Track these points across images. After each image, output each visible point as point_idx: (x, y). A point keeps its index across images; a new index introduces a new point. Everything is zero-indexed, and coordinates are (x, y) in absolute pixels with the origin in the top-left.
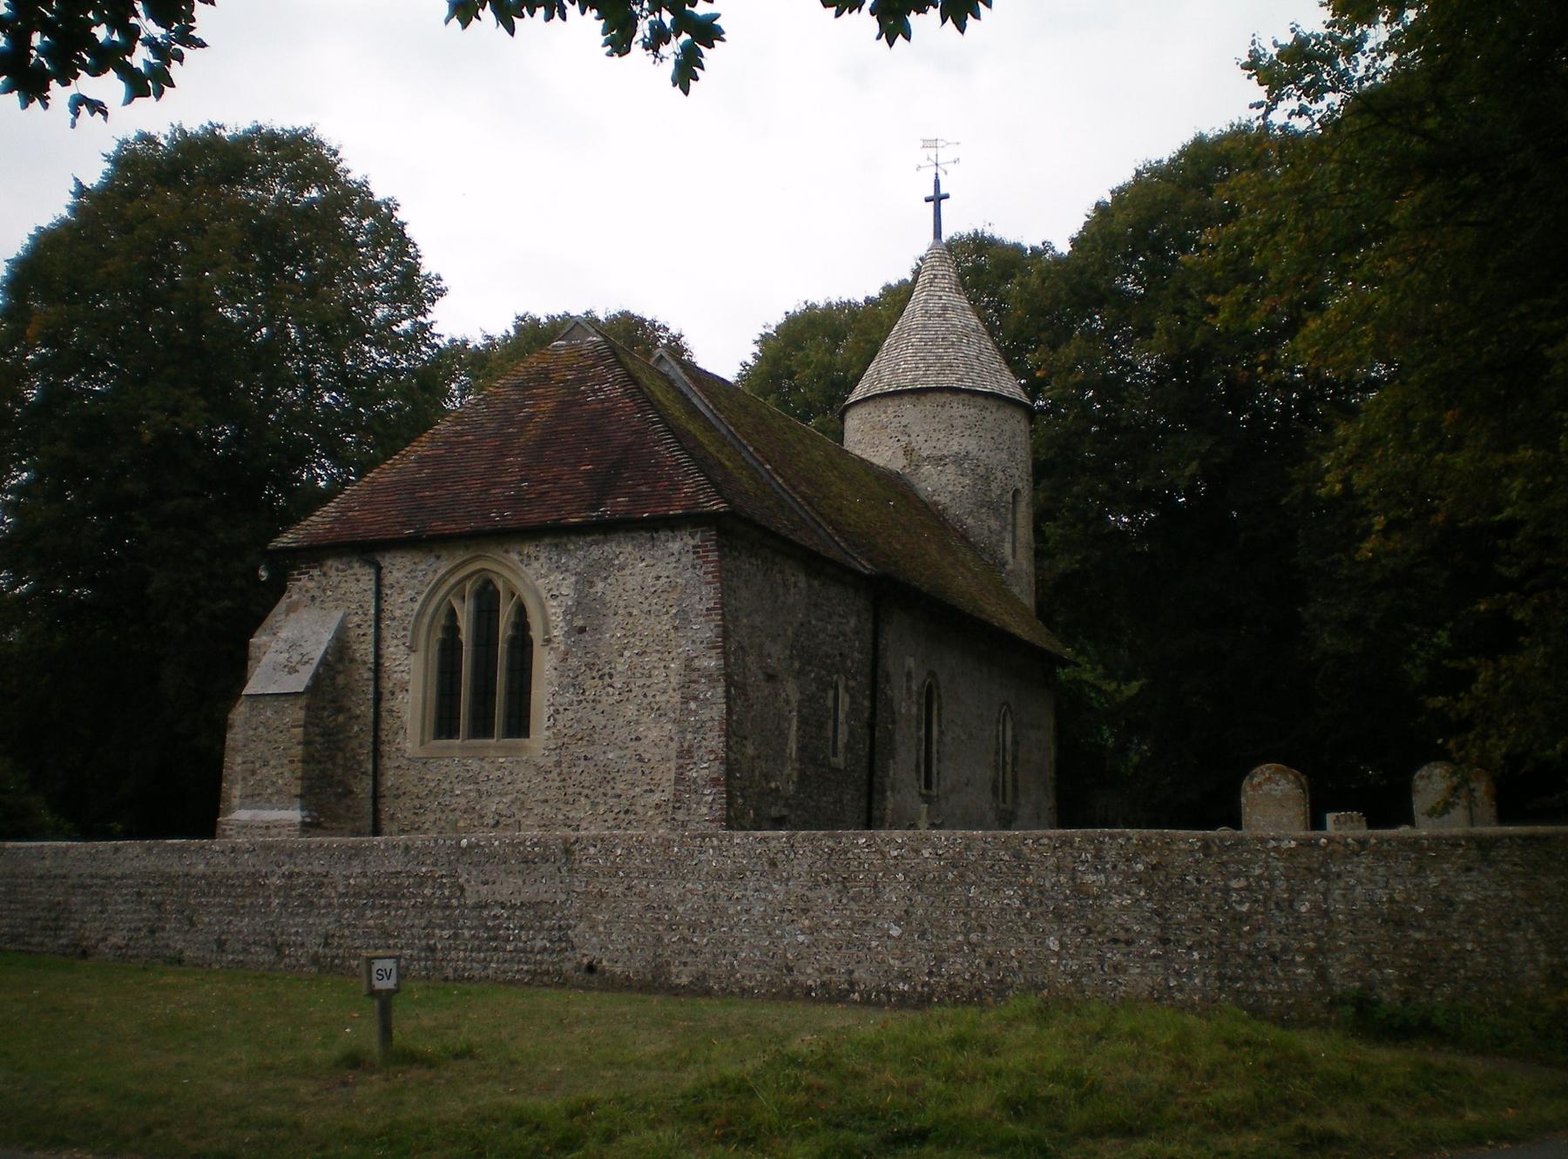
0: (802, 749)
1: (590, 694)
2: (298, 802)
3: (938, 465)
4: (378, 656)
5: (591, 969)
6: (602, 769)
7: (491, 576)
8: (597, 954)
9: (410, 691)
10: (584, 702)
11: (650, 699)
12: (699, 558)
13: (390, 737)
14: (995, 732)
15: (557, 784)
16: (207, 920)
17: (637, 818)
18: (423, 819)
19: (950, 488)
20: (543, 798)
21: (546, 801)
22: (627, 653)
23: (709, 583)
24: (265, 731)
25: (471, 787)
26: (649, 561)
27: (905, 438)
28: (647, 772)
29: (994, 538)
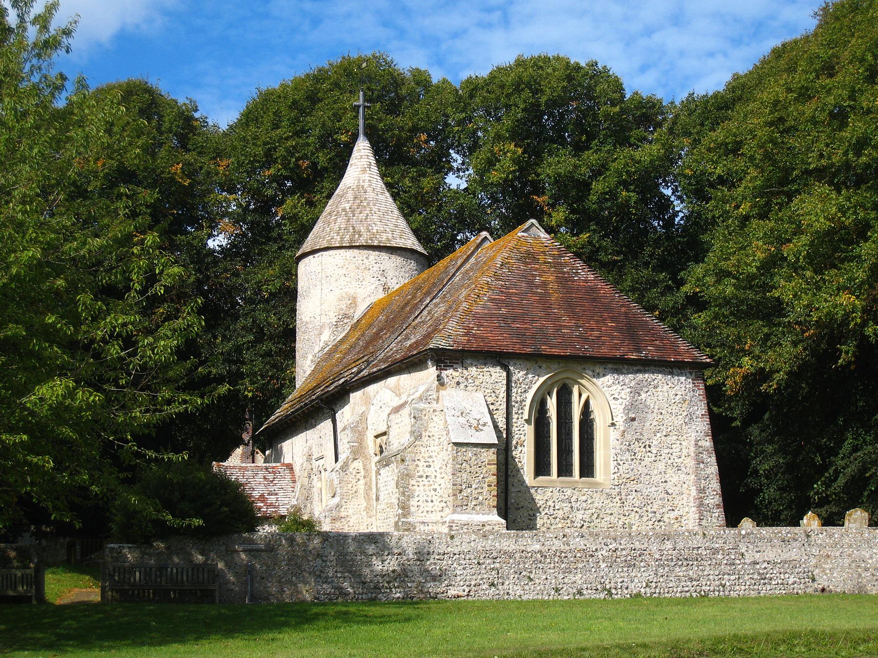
1: (639, 457)
5: (823, 590)
7: (568, 381)
8: (826, 584)
11: (672, 461)
17: (665, 524)
20: (610, 512)
21: (611, 514)
23: (701, 400)
24: (468, 467)
28: (671, 499)
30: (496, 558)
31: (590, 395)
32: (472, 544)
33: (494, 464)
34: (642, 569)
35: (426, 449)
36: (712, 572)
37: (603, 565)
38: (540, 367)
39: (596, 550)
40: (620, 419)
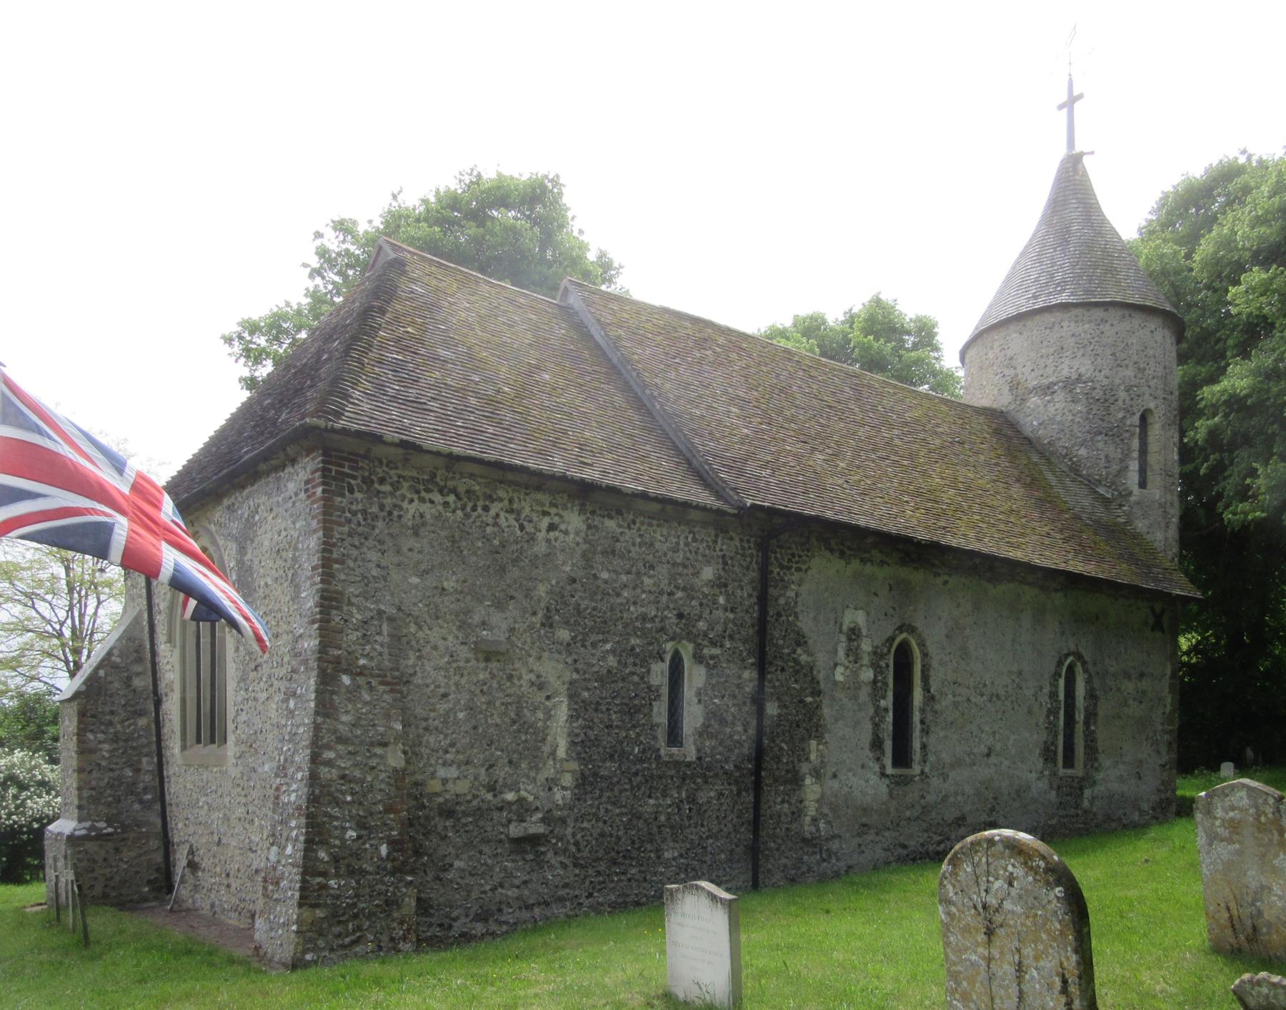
0: (582, 746)
3: (1046, 394)
14: (1046, 690)
19: (1058, 418)
27: (1012, 372)
29: (1115, 467)
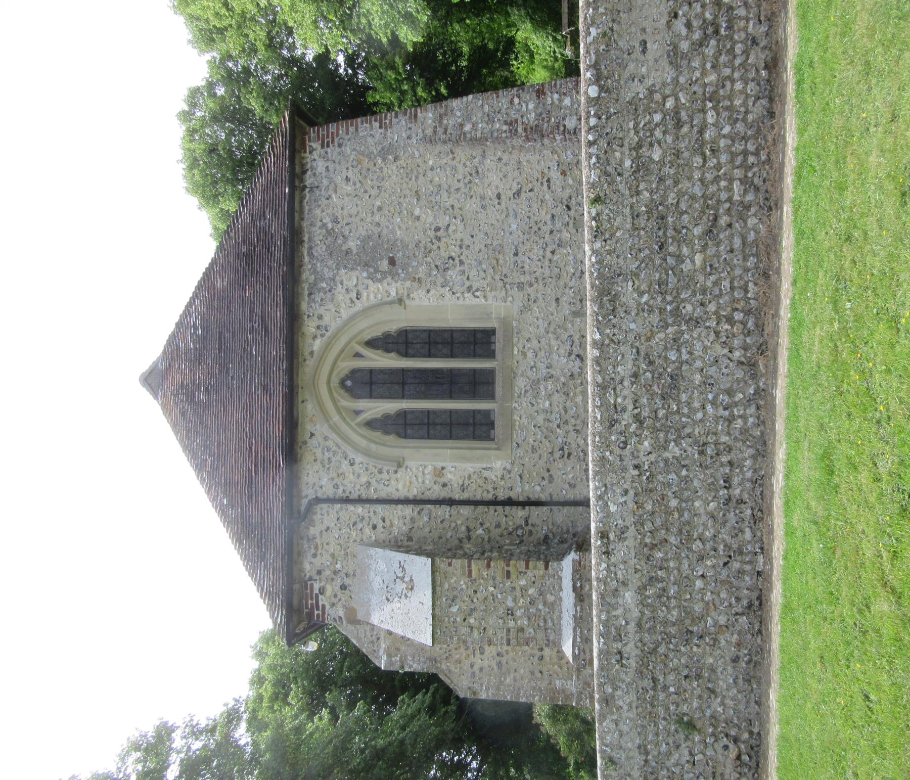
1: (454, 251)
2: (553, 565)
4: (406, 501)
6: (526, 236)
7: (335, 381)
9: (444, 464)
10: (462, 257)
11: (461, 185)
12: (333, 141)
13: (490, 488)
15: (541, 287)
16: (699, 584)
18: (574, 446)
21: (557, 300)
22: (417, 212)
24: (475, 614)
25: (542, 387)
26: (331, 192)
28: (530, 186)
30: (654, 680)
31: (356, 340)
32: (625, 728)
33: (470, 566)
34: (685, 357)
35: (454, 651)
36: (697, 175)
37: (674, 450)
38: (312, 435)
39: (636, 467)
40: (393, 289)
